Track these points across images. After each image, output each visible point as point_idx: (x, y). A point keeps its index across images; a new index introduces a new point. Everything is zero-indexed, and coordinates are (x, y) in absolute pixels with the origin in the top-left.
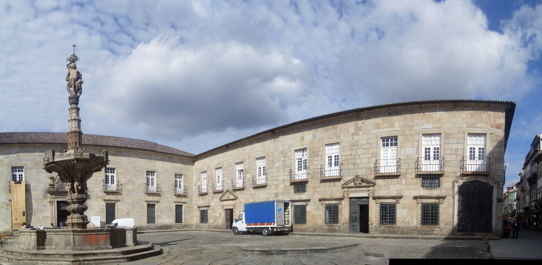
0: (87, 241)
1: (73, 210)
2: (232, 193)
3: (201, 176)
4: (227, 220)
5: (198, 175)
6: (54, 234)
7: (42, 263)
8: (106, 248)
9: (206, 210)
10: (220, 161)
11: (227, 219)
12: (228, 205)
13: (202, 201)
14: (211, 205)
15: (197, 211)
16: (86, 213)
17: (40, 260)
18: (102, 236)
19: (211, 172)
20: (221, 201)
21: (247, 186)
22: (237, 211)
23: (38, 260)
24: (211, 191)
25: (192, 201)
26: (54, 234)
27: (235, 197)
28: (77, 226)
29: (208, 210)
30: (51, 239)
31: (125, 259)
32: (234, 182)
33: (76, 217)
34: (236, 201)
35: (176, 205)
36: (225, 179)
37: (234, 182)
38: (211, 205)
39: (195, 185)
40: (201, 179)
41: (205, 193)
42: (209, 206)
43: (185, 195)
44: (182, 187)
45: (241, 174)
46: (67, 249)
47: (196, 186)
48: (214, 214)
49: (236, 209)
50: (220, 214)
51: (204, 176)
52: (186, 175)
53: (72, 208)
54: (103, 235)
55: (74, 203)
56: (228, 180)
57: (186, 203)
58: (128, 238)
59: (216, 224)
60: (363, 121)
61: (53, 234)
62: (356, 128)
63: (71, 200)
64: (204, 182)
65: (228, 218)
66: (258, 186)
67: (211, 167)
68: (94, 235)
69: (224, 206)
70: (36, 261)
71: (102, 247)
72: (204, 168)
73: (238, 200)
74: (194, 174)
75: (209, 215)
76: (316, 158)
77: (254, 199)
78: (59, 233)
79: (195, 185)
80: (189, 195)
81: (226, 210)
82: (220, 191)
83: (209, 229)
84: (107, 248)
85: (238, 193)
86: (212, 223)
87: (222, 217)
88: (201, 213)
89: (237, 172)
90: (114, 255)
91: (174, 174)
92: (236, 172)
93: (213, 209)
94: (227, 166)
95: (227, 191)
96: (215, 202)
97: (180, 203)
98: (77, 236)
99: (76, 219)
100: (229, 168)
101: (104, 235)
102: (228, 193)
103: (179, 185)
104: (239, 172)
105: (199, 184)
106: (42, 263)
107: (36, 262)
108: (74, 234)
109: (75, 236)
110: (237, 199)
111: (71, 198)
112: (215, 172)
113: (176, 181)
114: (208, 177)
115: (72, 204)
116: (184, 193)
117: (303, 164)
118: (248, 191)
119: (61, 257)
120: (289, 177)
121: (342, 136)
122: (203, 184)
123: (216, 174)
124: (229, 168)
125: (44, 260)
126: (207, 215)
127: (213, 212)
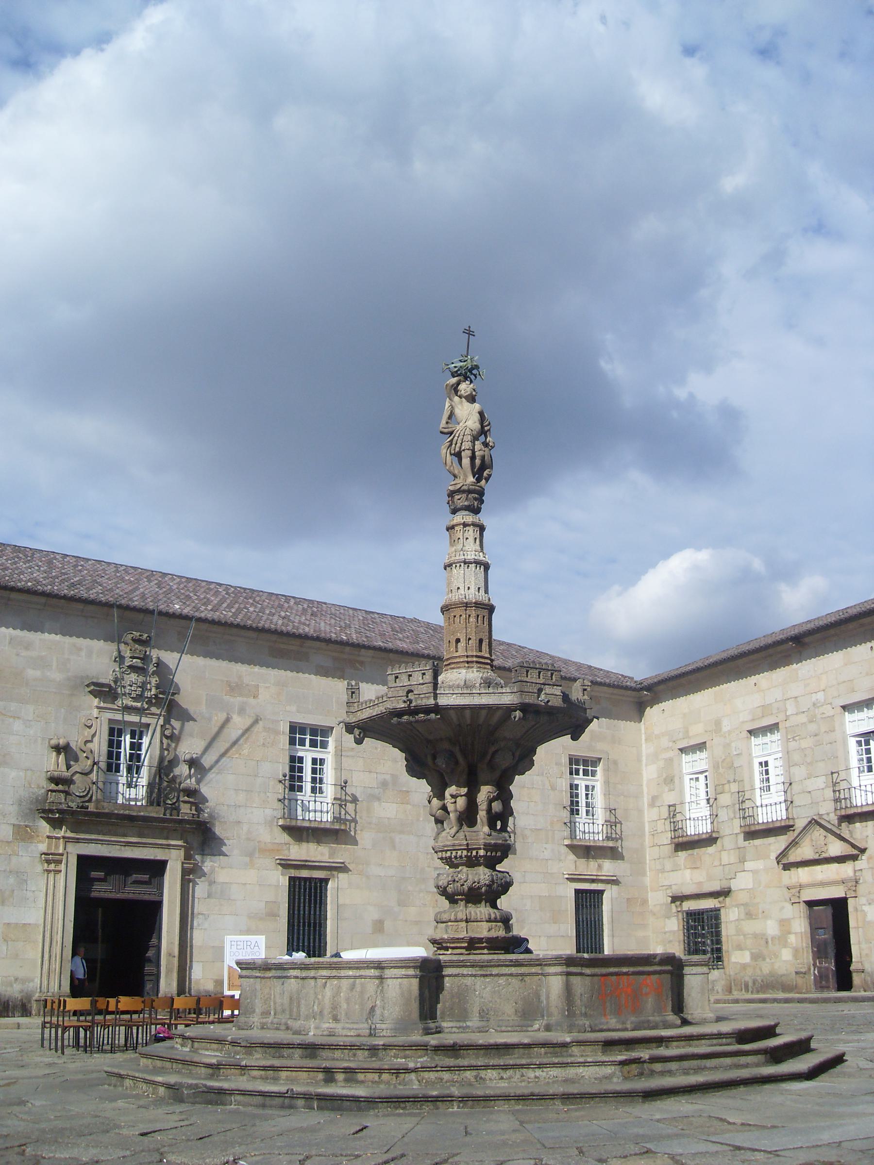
0: (609, 998)
1: (470, 889)
2: (835, 829)
3: (680, 765)
4: (819, 951)
5: (666, 760)
6: (475, 976)
7: (502, 1078)
8: (664, 1025)
9: (711, 910)
11: (818, 947)
12: (823, 884)
13: (688, 872)
14: (733, 888)
15: (669, 918)
16: (503, 902)
17: (494, 1067)
18: (648, 981)
19: (729, 745)
20: (787, 867)
22: (865, 908)
23: (486, 1067)
24: (731, 828)
25: (644, 874)
26: (475, 976)
27: (853, 846)
28: (486, 951)
29: (722, 911)
30: (462, 995)
31: (759, 1056)
32: (843, 785)
33: (485, 916)
35: (577, 892)
36: (799, 773)
37: (843, 785)
38: (734, 885)
39: (652, 804)
40: (681, 779)
41: (704, 836)
42: (725, 893)
43: (612, 848)
44: (600, 815)
46: (529, 1029)
47: (656, 810)
48: (751, 927)
49: (862, 900)
50: (784, 923)
51: (699, 761)
52: (615, 763)
53: (469, 883)
54: (652, 977)
55: (472, 862)
57: (615, 882)
58: (694, 994)
59: (766, 970)
61: (471, 975)
63: (465, 853)
64: (693, 791)
65: (825, 942)
67: (726, 726)
68: (625, 977)
69: (801, 887)
70: (474, 1073)
71: (651, 1018)
72: (691, 734)
73: (870, 858)
74: (644, 758)
75: (727, 931)
78: (495, 971)
79: (652, 805)
80: (627, 846)
81: (810, 904)
82: (778, 824)
83: (730, 991)
84: (667, 1026)
86: (744, 966)
87: (792, 939)
88: (688, 922)
89: (852, 742)
90: (715, 1045)
91: (565, 760)
93: (745, 905)
94: (803, 718)
95: (814, 823)
96: (755, 872)
97: (593, 881)
98: (579, 978)
99: (485, 925)
100: (812, 727)
101: (654, 977)
102: (818, 834)
103: (587, 805)
104: (859, 743)
105: (669, 798)
106: (502, 1078)
107: (476, 1077)
108: (803, 934)
109: (572, 978)
111: (467, 845)
112: (749, 748)
113: (573, 787)
114: (716, 766)
115: (465, 869)
116: (608, 838)
119: (556, 1055)
122: (688, 799)
123: (750, 755)
124: (812, 727)
125: (514, 1067)
126: (718, 934)
127: (749, 915)
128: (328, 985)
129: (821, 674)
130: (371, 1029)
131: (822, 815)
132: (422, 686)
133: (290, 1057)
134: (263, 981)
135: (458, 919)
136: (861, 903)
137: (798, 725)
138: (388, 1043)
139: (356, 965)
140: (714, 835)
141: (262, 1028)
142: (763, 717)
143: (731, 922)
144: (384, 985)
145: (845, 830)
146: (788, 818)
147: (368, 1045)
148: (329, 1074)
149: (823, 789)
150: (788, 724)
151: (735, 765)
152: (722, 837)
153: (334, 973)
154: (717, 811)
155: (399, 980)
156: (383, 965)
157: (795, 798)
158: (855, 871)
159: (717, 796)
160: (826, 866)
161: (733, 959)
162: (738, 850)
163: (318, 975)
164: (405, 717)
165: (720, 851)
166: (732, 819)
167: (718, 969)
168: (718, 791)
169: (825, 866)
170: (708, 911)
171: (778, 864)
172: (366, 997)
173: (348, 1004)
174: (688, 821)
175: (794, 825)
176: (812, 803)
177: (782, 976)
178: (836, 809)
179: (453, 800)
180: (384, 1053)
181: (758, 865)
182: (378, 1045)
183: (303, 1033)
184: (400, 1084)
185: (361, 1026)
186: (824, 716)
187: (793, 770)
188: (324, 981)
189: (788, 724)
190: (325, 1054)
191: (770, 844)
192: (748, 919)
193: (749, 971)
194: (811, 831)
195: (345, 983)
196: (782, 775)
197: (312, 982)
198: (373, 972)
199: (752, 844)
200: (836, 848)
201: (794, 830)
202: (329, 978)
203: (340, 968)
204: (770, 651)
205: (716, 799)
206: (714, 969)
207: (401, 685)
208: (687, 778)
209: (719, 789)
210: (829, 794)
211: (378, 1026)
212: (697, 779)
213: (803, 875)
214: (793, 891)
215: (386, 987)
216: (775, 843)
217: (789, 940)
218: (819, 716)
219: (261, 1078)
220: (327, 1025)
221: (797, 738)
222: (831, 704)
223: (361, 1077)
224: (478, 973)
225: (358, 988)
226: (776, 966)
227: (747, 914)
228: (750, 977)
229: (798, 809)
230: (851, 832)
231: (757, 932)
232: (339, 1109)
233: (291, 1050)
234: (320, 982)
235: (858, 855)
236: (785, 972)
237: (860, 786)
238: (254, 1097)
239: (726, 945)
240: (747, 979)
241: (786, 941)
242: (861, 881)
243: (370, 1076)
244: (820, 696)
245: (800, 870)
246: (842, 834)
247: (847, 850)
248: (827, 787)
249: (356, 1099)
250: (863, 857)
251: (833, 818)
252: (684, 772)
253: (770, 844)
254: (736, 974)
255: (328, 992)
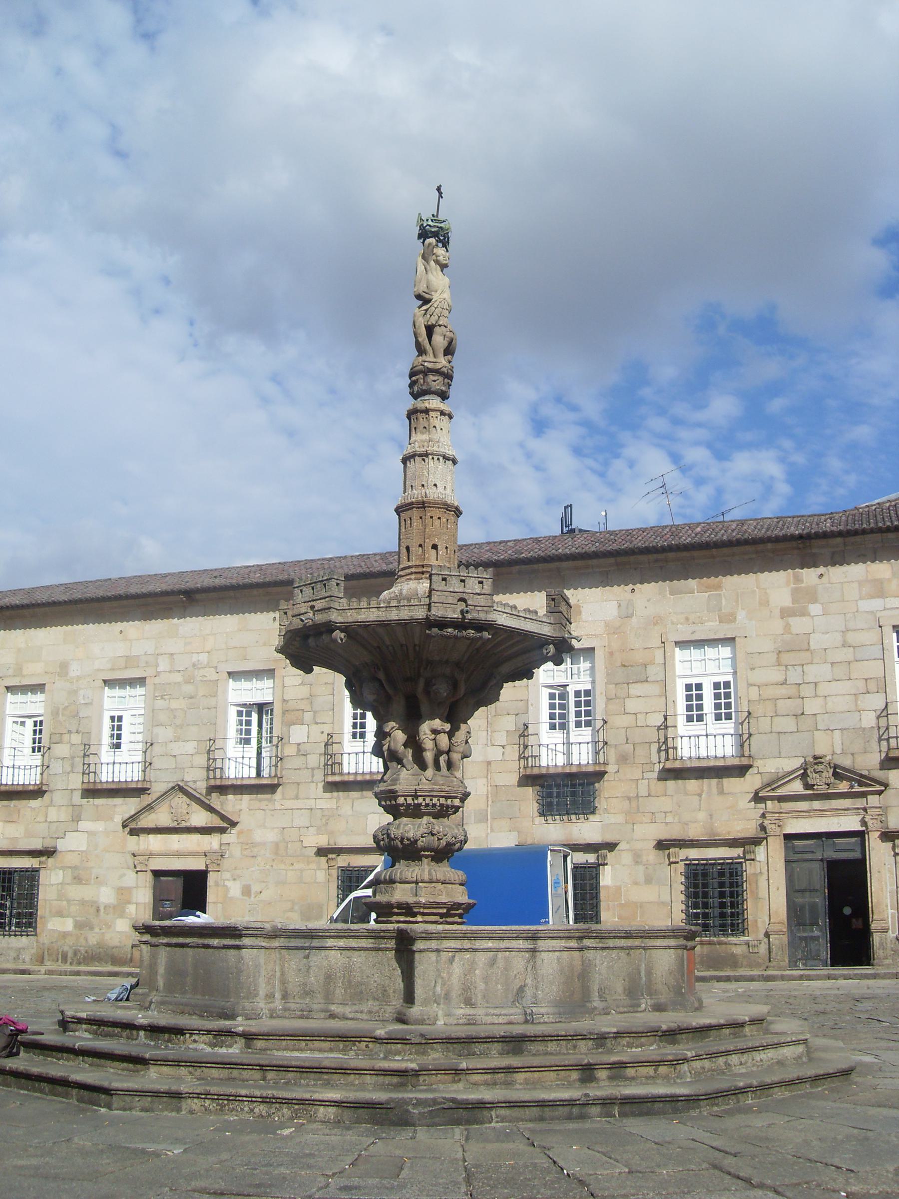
9: (27, 870)
10: (135, 652)
12: (179, 854)
19: (76, 692)
20: (134, 832)
21: (289, 776)
27: (223, 818)
29: (42, 873)
34: (224, 836)
38: (61, 845)
42: (48, 852)
45: (248, 723)
48: (76, 892)
51: (35, 704)
56: (177, 739)
60: (821, 570)
62: (795, 592)
66: (346, 778)
67: (75, 670)
69: (151, 855)
72: (25, 672)
73: (240, 833)
76: (636, 689)
77: (331, 833)
81: (157, 874)
85: (231, 804)
86: (65, 935)
87: (131, 909)
89: (233, 712)
92: (226, 713)
93: (75, 868)
94: (178, 678)
96: (90, 833)
100: (188, 689)
102: (180, 801)
104: (240, 713)
110: (234, 831)
117: (572, 709)
118: (297, 798)
120: (513, 753)
121: (741, 615)
123: (102, 706)
124: (188, 689)
127: (78, 880)
128: (457, 959)
129: (208, 635)
130: (526, 1014)
131: (187, 782)
132: (479, 597)
133: (485, 1054)
134: (268, 952)
135: (434, 879)
136: (224, 877)
137: (170, 684)
138: (622, 1030)
139: (502, 935)
140: (44, 788)
141: (272, 1017)
142: (126, 668)
143: (52, 885)
144: (537, 959)
145: (216, 801)
146: (144, 780)
147: (597, 1034)
148: (587, 1072)
149: (192, 755)
150: (157, 680)
151: (81, 715)
152: (52, 791)
153: (467, 944)
154: (49, 761)
155: (557, 954)
156: (539, 935)
157: (155, 760)
158: (221, 844)
159: (52, 746)
160: (185, 836)
161: (50, 926)
162: (71, 807)
163: (444, 946)
164: (450, 630)
165: (47, 806)
166: (69, 773)
167: (28, 935)
168: (54, 740)
169: (184, 836)
170: (21, 871)
171: (124, 826)
172: (512, 974)
173: (486, 983)
174: (16, 770)
175: (149, 789)
176: (176, 768)
177: (113, 948)
178: (208, 778)
179: (433, 736)
180: (613, 1042)
181: (99, 826)
182: (609, 1033)
183: (427, 1022)
184: (677, 1077)
185: (512, 1011)
186: (205, 679)
187: (156, 730)
188: (450, 954)
189: (157, 680)
190: (533, 1047)
191: (115, 806)
192: (76, 884)
193: (70, 941)
194: (172, 797)
195: (482, 958)
196: (140, 733)
197: (433, 956)
198: (521, 944)
199: (91, 803)
200: (200, 818)
201: (149, 794)
202: (460, 950)
203: (475, 939)
204: (150, 600)
205: (49, 749)
206: (22, 935)
207: (451, 590)
208: (9, 721)
209: (56, 738)
210: (202, 760)
211: (534, 1010)
212: (23, 724)
213: (154, 842)
214: (141, 858)
215: (539, 962)
216: (122, 804)
217: (127, 910)
218: (199, 679)
219: (486, 1084)
220: (461, 1011)
221: (166, 697)
222: (216, 667)
223: (630, 1072)
224: (601, 945)
225: (501, 963)
226: (107, 937)
227: (75, 878)
228: (71, 947)
229: (158, 772)
230: (222, 804)
231: (87, 899)
232: (649, 1113)
233: (485, 1045)
234: (445, 956)
235: (228, 828)
236: (118, 944)
237: (243, 757)
238: (526, 1109)
239: (42, 910)
240: (66, 948)
241: (124, 911)
242: (227, 856)
243: (644, 1071)
244: (204, 658)
245: (151, 837)
246: (212, 805)
247: (217, 822)
248: (197, 753)
249: (673, 1099)
250: (233, 831)
251: (202, 786)
252: (7, 712)
253: (115, 806)
254: (52, 943)
255: (457, 969)
